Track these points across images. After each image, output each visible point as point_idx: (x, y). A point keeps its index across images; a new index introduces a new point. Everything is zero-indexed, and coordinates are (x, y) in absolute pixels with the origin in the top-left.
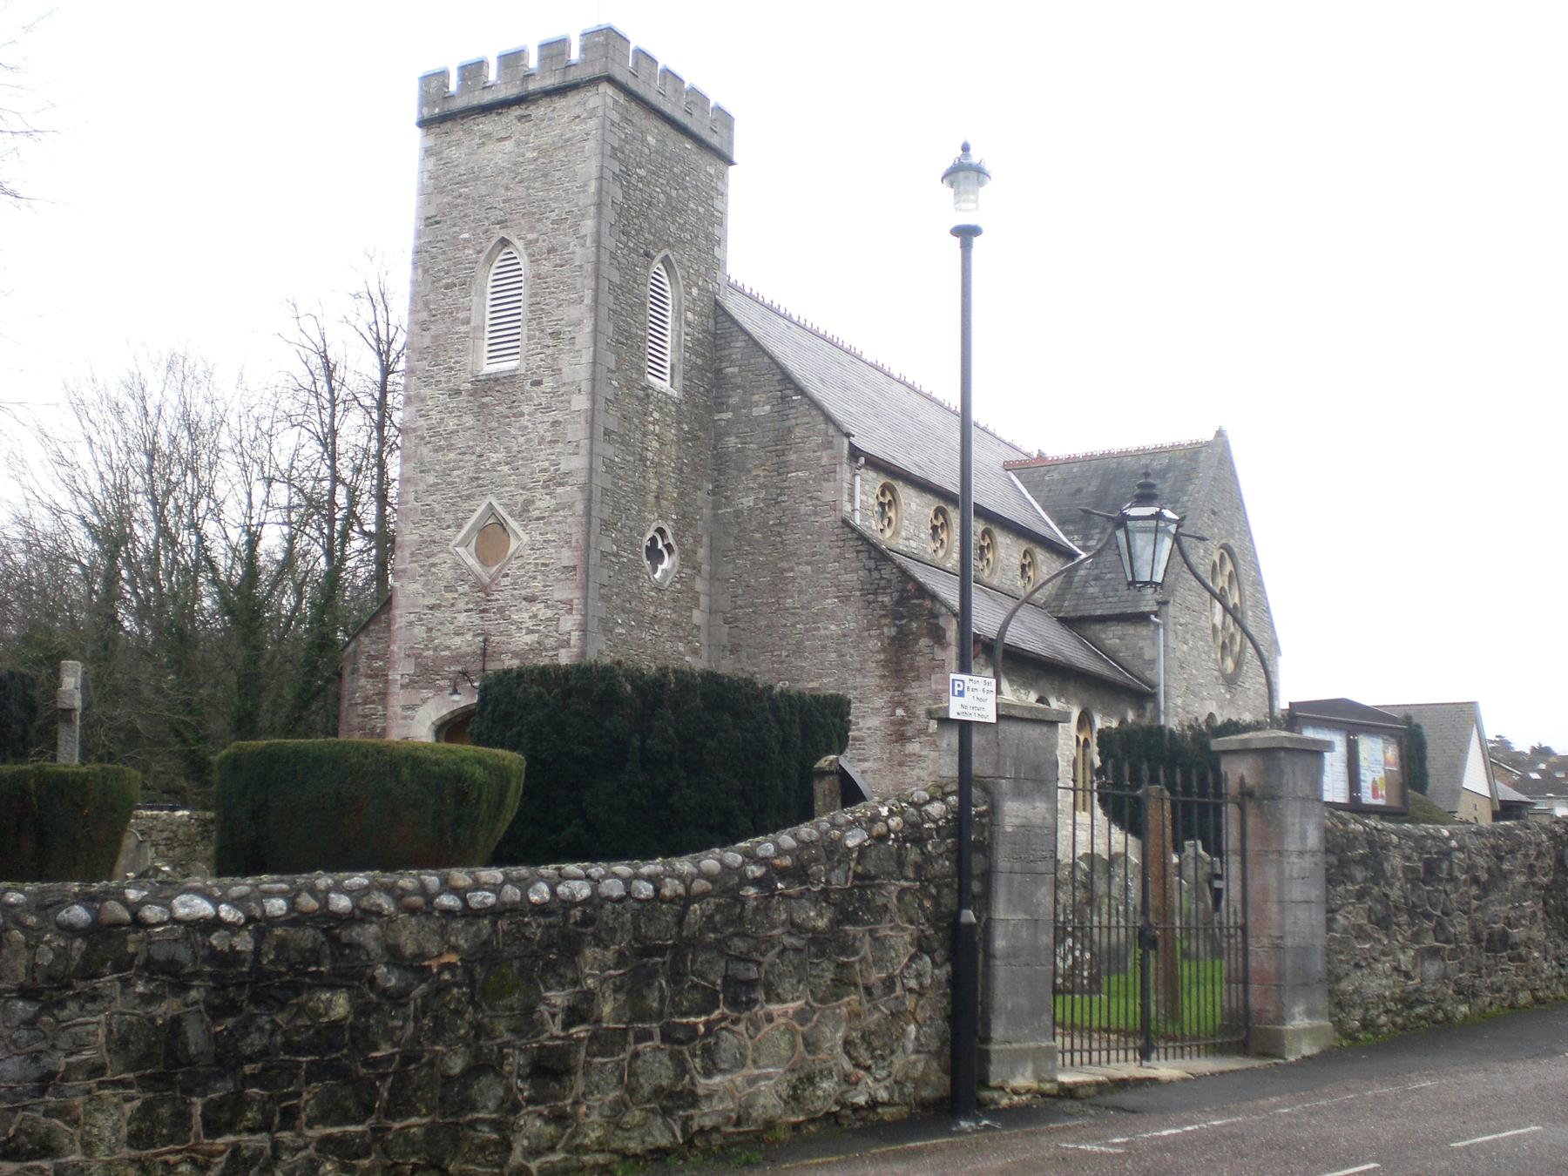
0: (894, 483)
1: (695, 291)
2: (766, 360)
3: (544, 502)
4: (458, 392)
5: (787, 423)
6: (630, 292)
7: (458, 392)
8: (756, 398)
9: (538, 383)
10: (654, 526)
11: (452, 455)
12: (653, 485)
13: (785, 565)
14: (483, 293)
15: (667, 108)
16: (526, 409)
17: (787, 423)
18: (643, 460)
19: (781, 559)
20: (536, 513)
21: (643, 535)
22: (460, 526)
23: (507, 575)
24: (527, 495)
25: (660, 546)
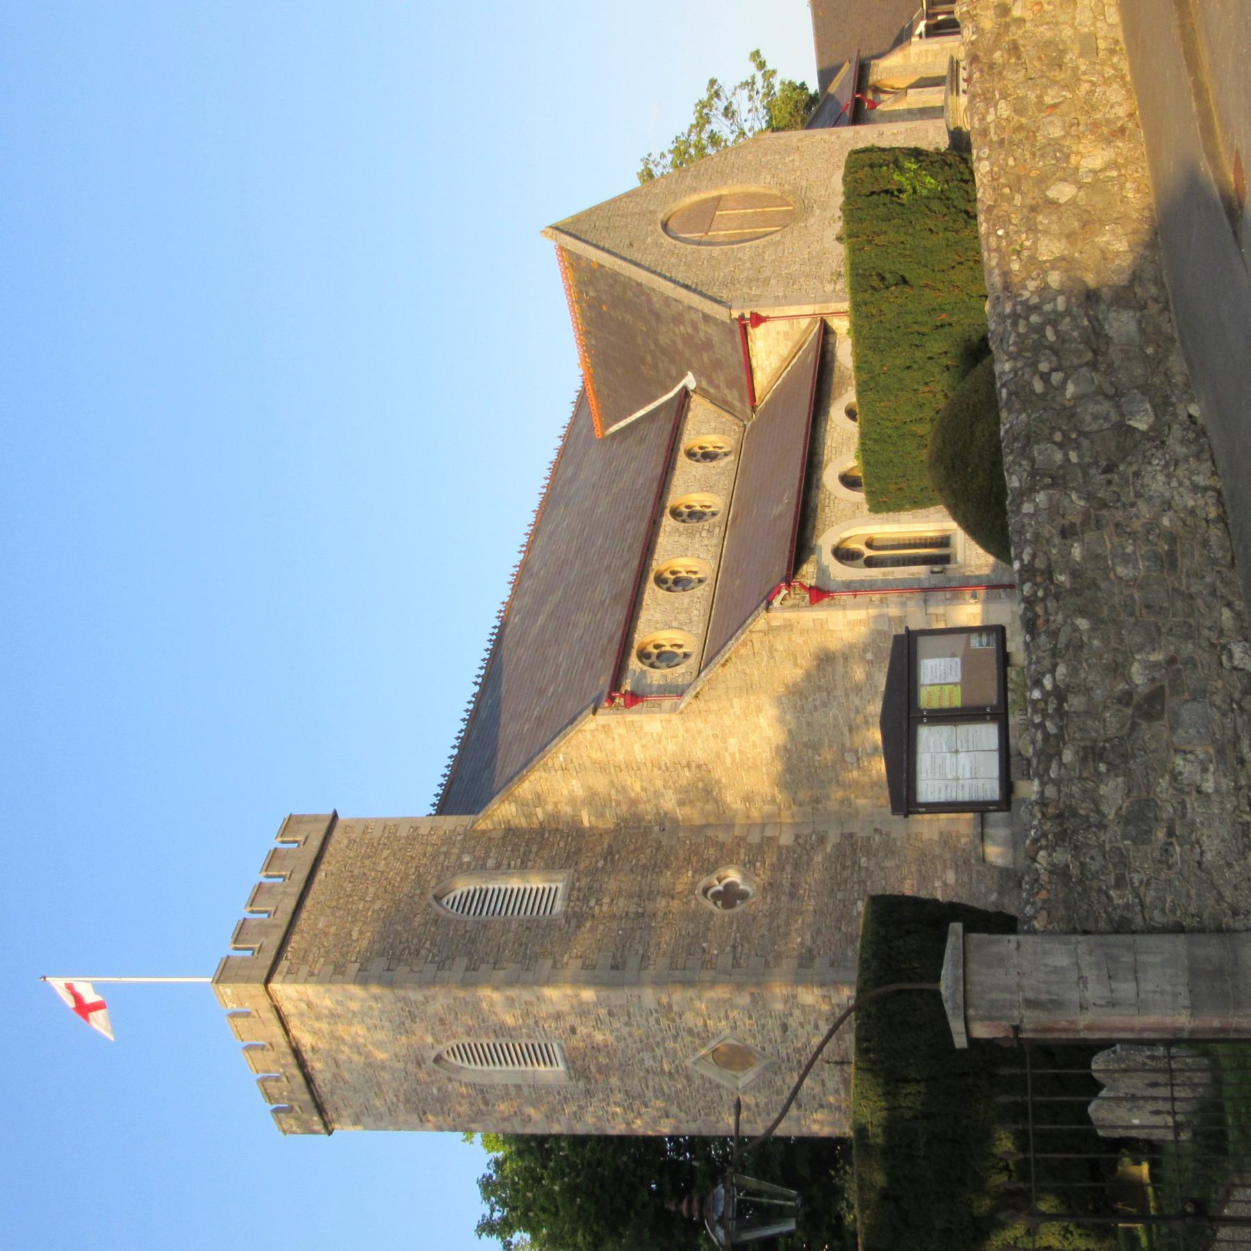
0: (636, 645)
8: (565, 792)
10: (701, 899)
13: (728, 760)
15: (290, 904)
17: (588, 764)
18: (639, 916)
21: (712, 914)
25: (720, 888)
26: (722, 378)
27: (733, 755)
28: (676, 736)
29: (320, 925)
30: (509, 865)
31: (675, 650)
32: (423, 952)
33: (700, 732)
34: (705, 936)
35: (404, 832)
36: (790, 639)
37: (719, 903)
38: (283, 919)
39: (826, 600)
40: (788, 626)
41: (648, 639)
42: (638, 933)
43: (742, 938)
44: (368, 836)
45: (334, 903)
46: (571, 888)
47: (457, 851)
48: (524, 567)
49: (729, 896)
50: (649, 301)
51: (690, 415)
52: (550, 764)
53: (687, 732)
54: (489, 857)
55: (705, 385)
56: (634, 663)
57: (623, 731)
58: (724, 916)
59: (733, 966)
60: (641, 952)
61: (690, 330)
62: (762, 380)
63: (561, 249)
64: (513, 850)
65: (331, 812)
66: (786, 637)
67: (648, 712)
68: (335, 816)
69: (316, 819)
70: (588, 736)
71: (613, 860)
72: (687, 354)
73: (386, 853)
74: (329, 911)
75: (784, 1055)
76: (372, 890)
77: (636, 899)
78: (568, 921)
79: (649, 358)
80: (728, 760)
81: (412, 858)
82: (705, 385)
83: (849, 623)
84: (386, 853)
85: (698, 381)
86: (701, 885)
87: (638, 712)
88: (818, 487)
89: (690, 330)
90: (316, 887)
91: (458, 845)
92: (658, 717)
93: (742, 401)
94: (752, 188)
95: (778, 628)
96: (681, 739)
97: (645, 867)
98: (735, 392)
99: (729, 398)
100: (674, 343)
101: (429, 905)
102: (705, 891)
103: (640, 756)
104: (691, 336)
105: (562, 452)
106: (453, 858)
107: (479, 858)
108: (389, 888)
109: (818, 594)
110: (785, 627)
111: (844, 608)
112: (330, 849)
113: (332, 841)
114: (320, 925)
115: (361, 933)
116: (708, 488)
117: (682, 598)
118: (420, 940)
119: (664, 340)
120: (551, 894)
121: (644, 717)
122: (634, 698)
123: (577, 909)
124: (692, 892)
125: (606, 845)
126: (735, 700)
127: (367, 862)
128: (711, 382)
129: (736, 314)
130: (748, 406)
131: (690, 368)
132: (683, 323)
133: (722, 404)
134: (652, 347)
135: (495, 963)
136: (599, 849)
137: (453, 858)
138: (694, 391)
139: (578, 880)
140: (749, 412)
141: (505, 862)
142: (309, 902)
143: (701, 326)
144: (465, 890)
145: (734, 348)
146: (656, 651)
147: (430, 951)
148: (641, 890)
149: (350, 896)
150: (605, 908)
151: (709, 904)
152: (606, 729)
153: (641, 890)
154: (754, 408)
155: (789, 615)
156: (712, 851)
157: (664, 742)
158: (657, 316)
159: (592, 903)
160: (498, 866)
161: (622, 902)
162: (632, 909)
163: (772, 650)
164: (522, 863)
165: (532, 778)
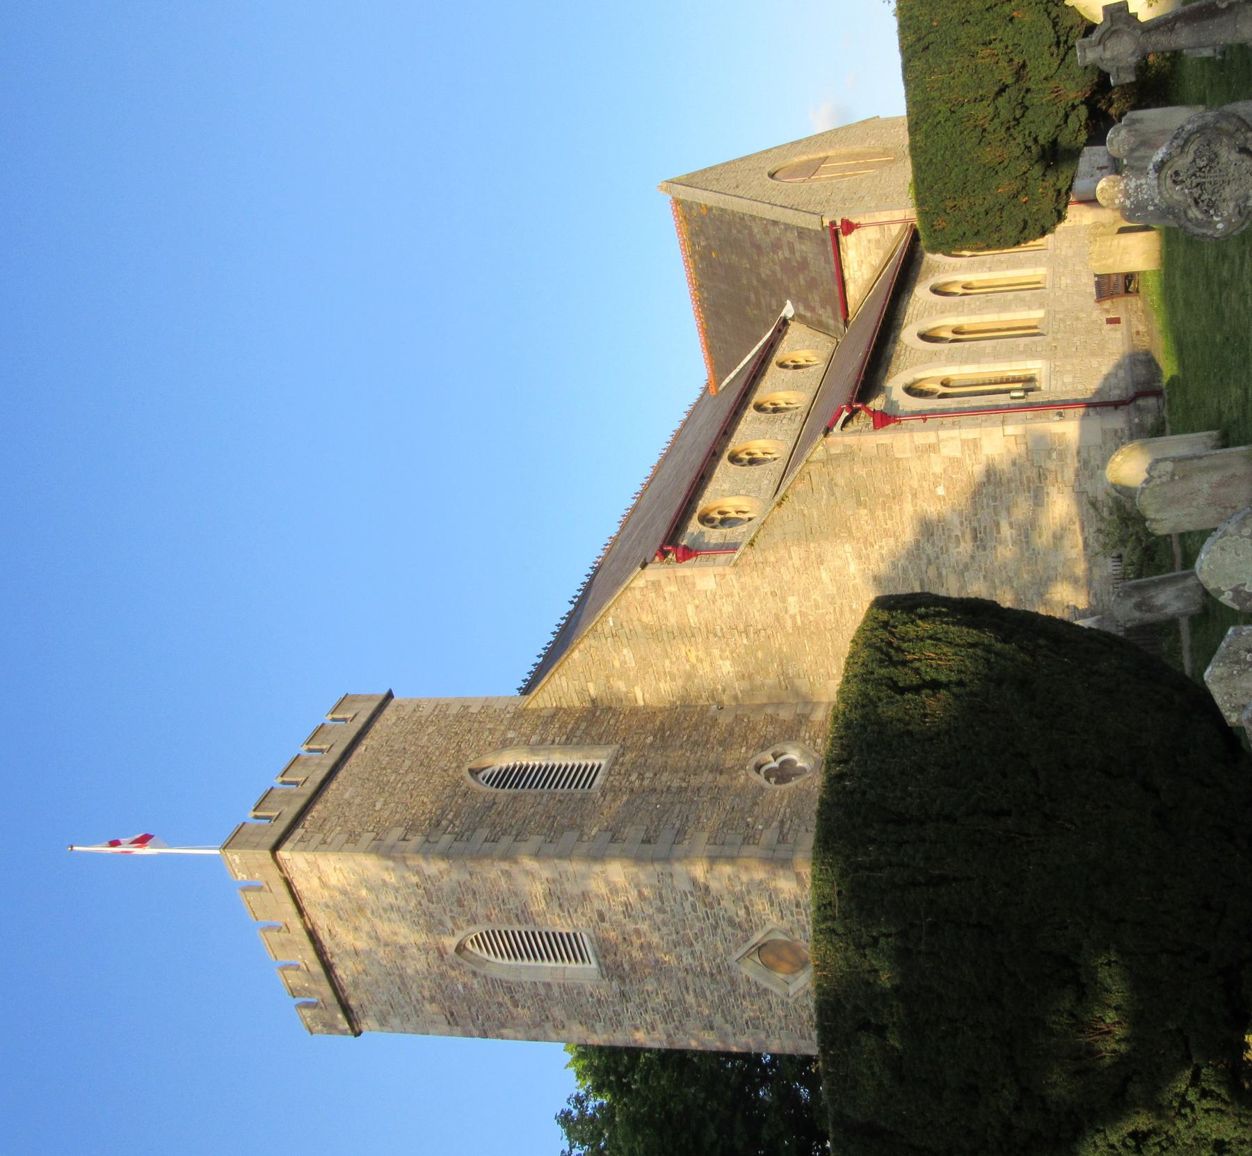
0: (699, 510)
4: (623, 994)
5: (639, 629)
7: (623, 994)
8: (617, 664)
10: (753, 775)
11: (690, 999)
12: (707, 777)
13: (789, 623)
15: (320, 775)
17: (639, 629)
18: (681, 790)
19: (783, 628)
20: (742, 912)
21: (762, 789)
22: (766, 991)
25: (775, 764)
26: (817, 298)
27: (793, 617)
28: (732, 595)
29: (347, 796)
30: (553, 742)
31: (741, 516)
32: (444, 823)
33: (757, 589)
34: (751, 811)
35: (453, 711)
36: (851, 470)
37: (772, 780)
38: (309, 788)
39: (892, 425)
40: (849, 454)
41: (713, 504)
42: (678, 807)
43: (792, 813)
44: (418, 714)
45: (366, 775)
46: (615, 761)
47: (503, 728)
48: (635, 509)
49: (784, 773)
50: (751, 234)
51: (786, 337)
52: (599, 629)
53: (743, 589)
54: (534, 733)
55: (802, 311)
56: (694, 526)
57: (673, 589)
58: (775, 791)
59: (779, 842)
60: (677, 826)
61: (787, 255)
62: (855, 293)
63: (677, 202)
64: (560, 727)
65: (385, 692)
66: (847, 469)
67: (700, 566)
68: (390, 696)
69: (370, 698)
70: (637, 594)
71: (663, 736)
72: (786, 281)
73: (431, 729)
74: (359, 782)
76: (408, 763)
77: (681, 774)
78: (604, 795)
79: (752, 296)
80: (789, 623)
81: (456, 733)
82: (802, 311)
83: (917, 448)
84: (431, 729)
85: (796, 308)
86: (754, 762)
87: (692, 566)
88: (895, 342)
89: (787, 255)
90: (353, 760)
91: (505, 722)
92: (711, 571)
93: (836, 319)
94: (858, 149)
95: (837, 457)
96: (736, 598)
97: (696, 743)
98: (829, 309)
99: (824, 319)
100: (774, 272)
101: (462, 778)
102: (758, 768)
103: (693, 620)
104: (788, 260)
105: (685, 424)
106: (498, 734)
107: (523, 735)
108: (426, 762)
109: (883, 420)
110: (846, 455)
111: (911, 430)
112: (377, 726)
113: (382, 718)
114: (347, 796)
115: (385, 803)
116: (795, 387)
117: (756, 470)
118: (443, 812)
119: (765, 272)
120: (594, 771)
121: (695, 570)
122: (687, 554)
123: (616, 783)
124: (743, 767)
125: (658, 723)
126: (794, 549)
127: (410, 737)
128: (808, 307)
129: (826, 223)
130: (841, 320)
131: (789, 296)
132: (780, 248)
133: (818, 326)
134: (755, 283)
135: (517, 836)
136: (649, 726)
137: (498, 734)
138: (793, 319)
139: (623, 754)
140: (842, 327)
141: (550, 738)
142: (342, 775)
143: (797, 246)
144: (504, 765)
145: (827, 261)
146: (719, 517)
147: (451, 822)
148: (688, 765)
149: (385, 768)
150: (646, 782)
151: (760, 779)
152: (656, 585)
153: (688, 765)
154: (846, 323)
155: (850, 440)
156: (770, 728)
157: (719, 603)
158: (758, 247)
159: (633, 778)
160: (542, 741)
161: (665, 777)
162: (676, 784)
163: (832, 485)
164: (568, 739)
165: (581, 646)
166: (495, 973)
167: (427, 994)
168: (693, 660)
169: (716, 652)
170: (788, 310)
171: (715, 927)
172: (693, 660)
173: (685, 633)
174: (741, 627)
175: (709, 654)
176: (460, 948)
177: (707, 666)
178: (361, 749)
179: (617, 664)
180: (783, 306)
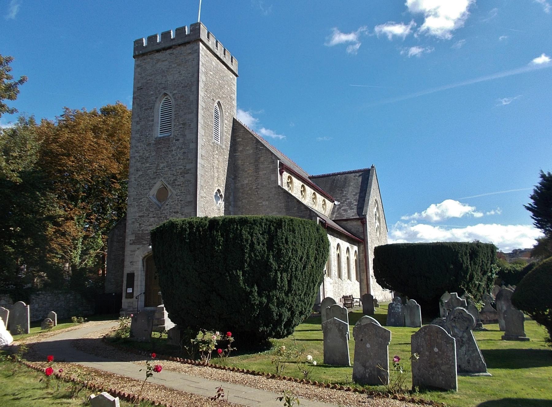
1: (227, 114)
2: (251, 136)
3: (181, 180)
6: (208, 110)
8: (248, 148)
9: (178, 140)
11: (148, 165)
12: (216, 175)
14: (158, 112)
16: (174, 148)
18: (213, 166)
20: (179, 183)
23: (167, 205)
24: (175, 178)
27: (262, 203)
28: (269, 185)
55: (337, 207)
75: (164, 212)
103: (261, 173)
161: (217, 162)
166: (157, 105)
167: (149, 81)
168: (249, 171)
169: (250, 179)
170: (336, 203)
171: (173, 175)
172: (249, 171)
173: (257, 169)
174: (258, 187)
175: (250, 177)
176: (165, 94)
177: (246, 175)
178: (225, 67)
179: (248, 148)
180: (338, 201)
